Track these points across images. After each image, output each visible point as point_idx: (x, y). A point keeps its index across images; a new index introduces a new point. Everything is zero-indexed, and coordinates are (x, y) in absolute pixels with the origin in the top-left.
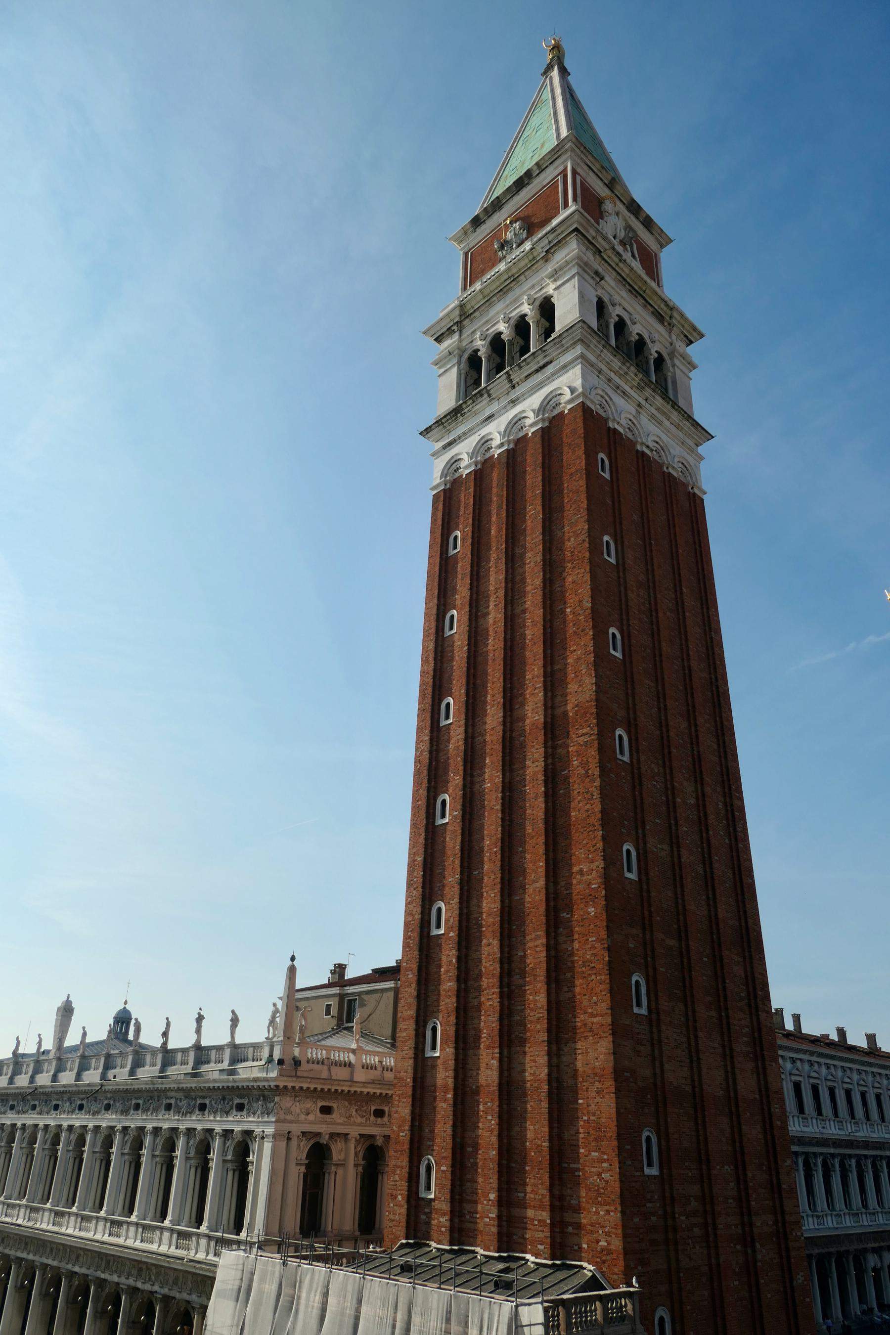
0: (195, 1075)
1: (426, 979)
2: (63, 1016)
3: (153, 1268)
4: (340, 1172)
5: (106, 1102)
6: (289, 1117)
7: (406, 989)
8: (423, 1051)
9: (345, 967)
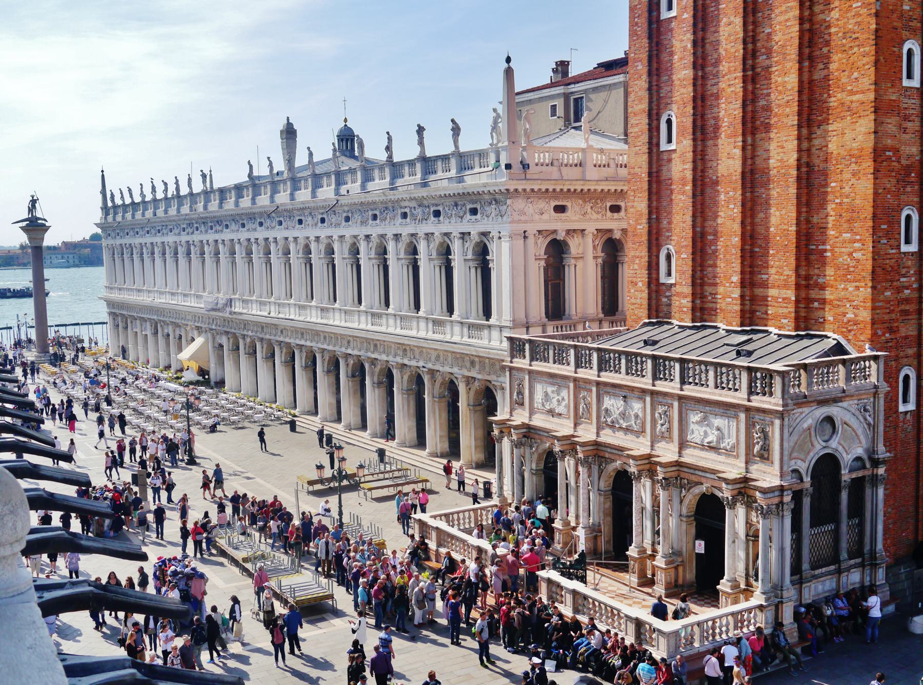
0: (425, 185)
1: (657, 69)
2: (286, 138)
3: (416, 349)
4: (580, 264)
5: (345, 215)
6: (523, 218)
7: (635, 82)
8: (658, 145)
9: (568, 64)
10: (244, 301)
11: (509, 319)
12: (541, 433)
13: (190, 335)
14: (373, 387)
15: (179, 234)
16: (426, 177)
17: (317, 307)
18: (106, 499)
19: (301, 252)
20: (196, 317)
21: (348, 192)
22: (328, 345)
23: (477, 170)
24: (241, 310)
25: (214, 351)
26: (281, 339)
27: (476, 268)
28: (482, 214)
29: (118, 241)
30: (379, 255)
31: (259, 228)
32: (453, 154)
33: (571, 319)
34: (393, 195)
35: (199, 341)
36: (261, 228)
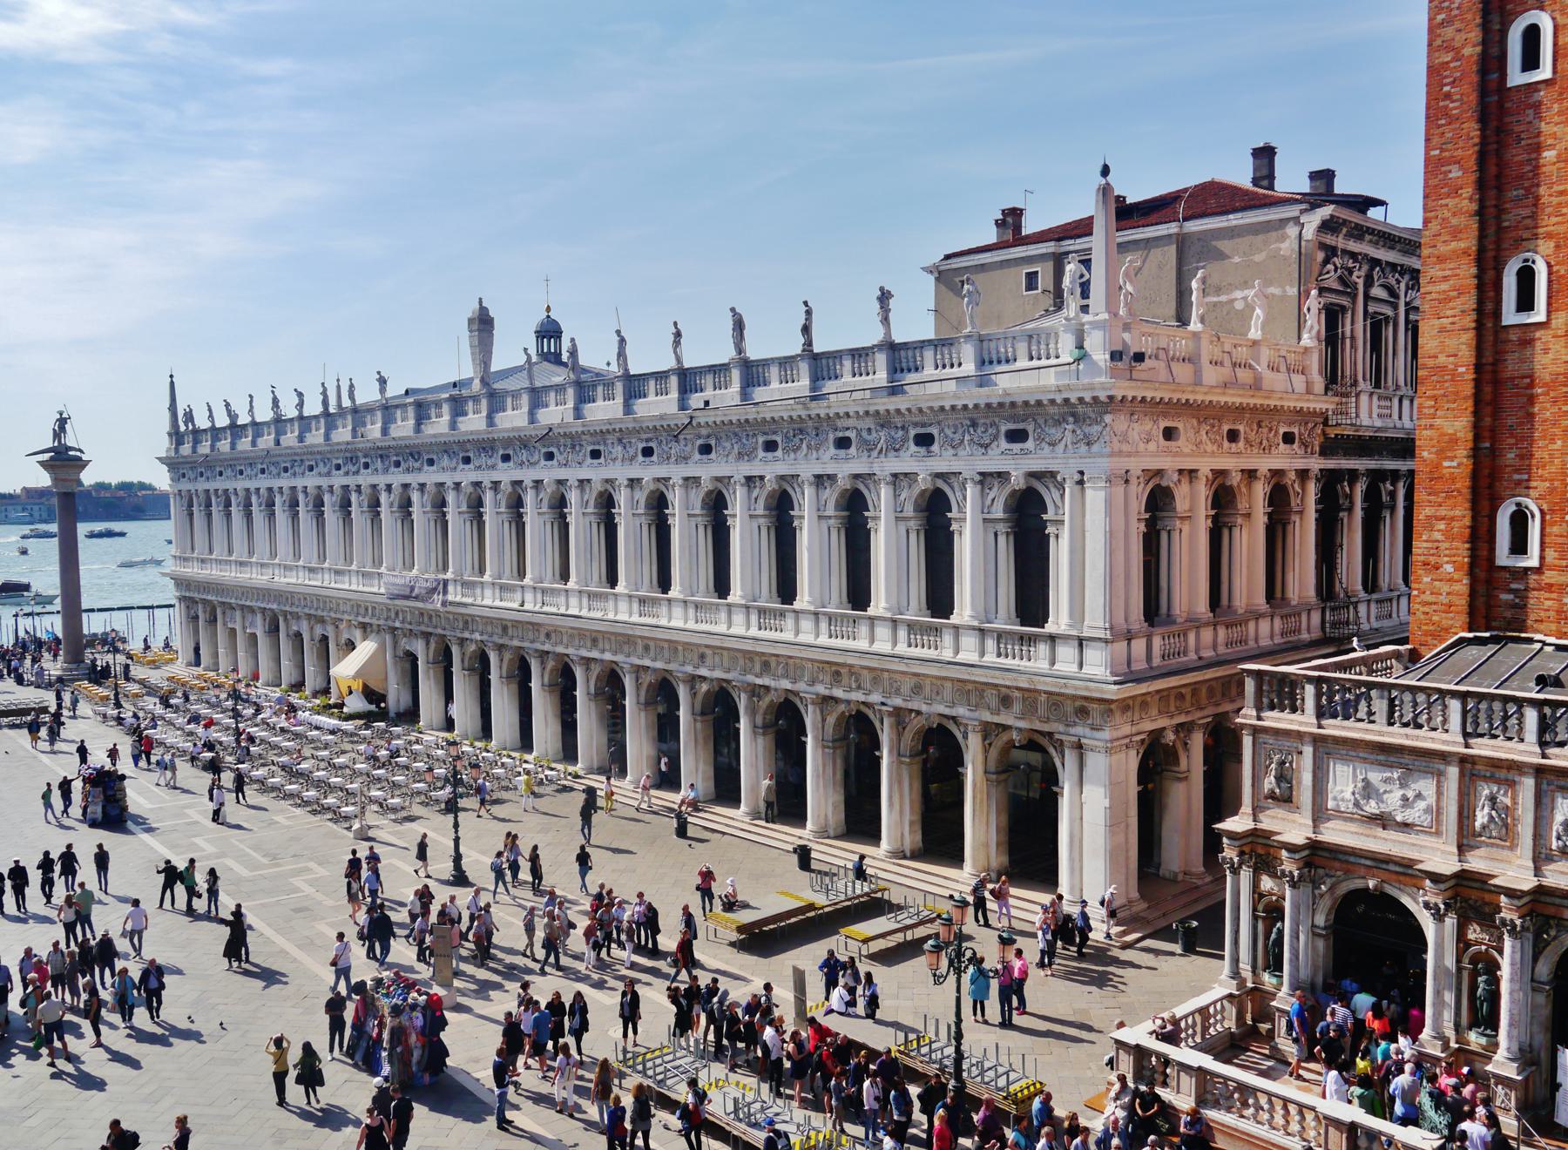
0: (895, 390)
1: (1498, 176)
2: (479, 330)
3: (865, 672)
4: (1186, 528)
5: (699, 442)
6: (1125, 448)
7: (1443, 202)
8: (1497, 314)
10: (465, 584)
11: (1101, 624)
12: (1352, 859)
13: (345, 636)
14: (755, 733)
15: (328, 474)
16: (898, 375)
17: (630, 596)
18: (414, 1007)
19: (592, 503)
20: (359, 607)
21: (707, 403)
22: (654, 660)
23: (1022, 363)
24: (458, 599)
25: (395, 664)
26: (547, 647)
27: (1008, 534)
28: (1040, 439)
29: (202, 485)
30: (602, 508)
31: (501, 465)
32: (879, 347)
33: (1174, 622)
34: (819, 409)
35: (366, 649)
36: (506, 465)
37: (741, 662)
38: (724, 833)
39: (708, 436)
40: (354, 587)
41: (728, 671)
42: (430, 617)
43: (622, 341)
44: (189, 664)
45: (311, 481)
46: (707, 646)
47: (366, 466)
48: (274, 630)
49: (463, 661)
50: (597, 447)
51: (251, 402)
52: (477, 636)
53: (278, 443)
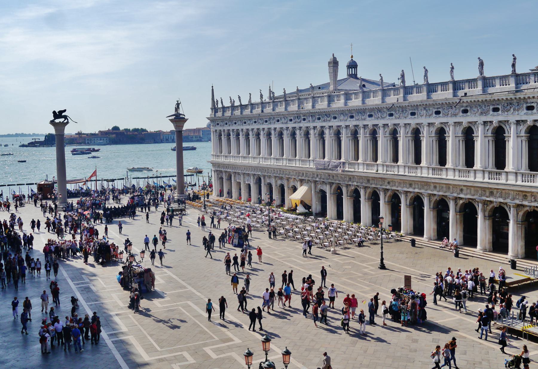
10: (350, 164)
13: (292, 184)
15: (286, 123)
19: (410, 132)
21: (466, 94)
26: (388, 187)
31: (368, 118)
37: (480, 192)
38: (473, 257)
39: (467, 106)
40: (297, 165)
41: (474, 195)
42: (333, 177)
43: (426, 71)
44: (218, 196)
45: (278, 126)
46: (464, 186)
47: (304, 120)
48: (259, 181)
49: (347, 193)
50: (414, 111)
51: (250, 96)
52: (355, 184)
53: (262, 111)
